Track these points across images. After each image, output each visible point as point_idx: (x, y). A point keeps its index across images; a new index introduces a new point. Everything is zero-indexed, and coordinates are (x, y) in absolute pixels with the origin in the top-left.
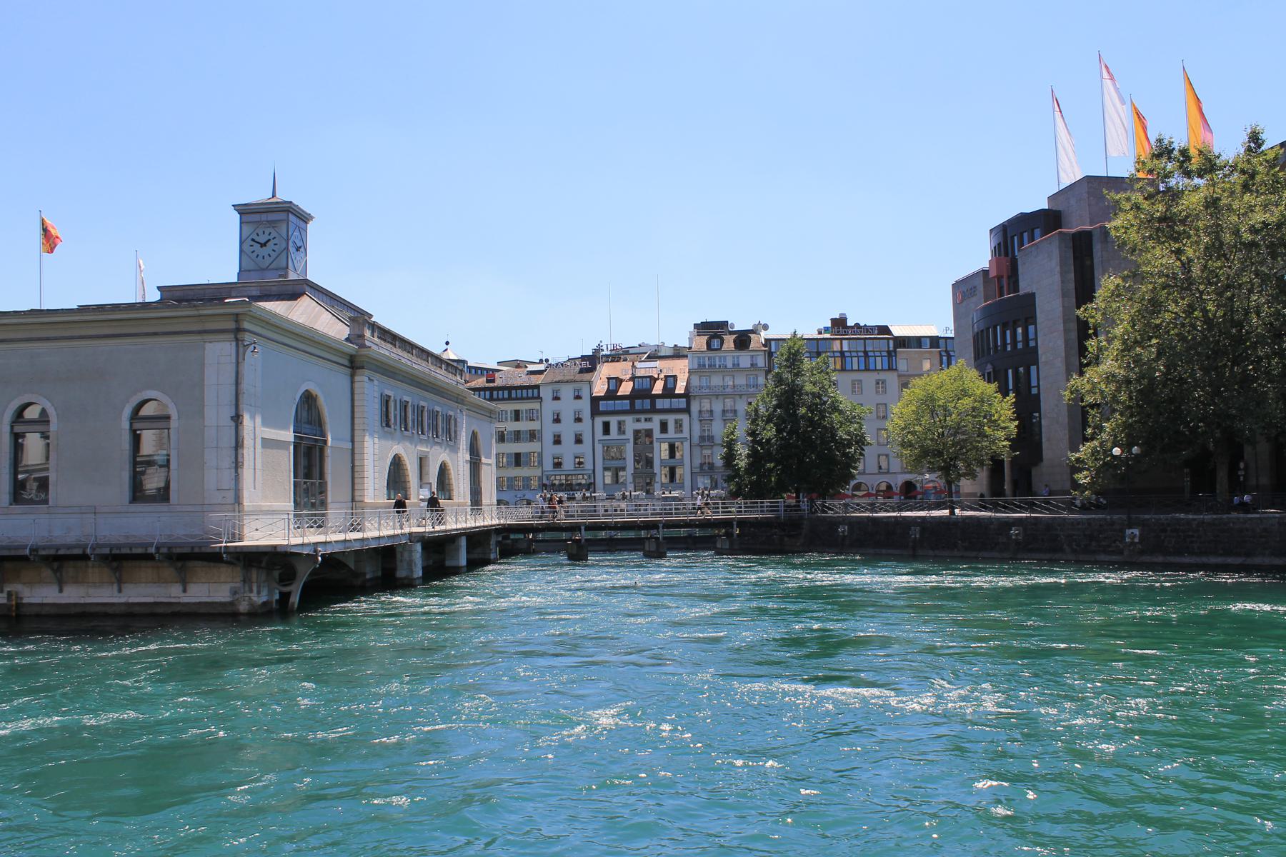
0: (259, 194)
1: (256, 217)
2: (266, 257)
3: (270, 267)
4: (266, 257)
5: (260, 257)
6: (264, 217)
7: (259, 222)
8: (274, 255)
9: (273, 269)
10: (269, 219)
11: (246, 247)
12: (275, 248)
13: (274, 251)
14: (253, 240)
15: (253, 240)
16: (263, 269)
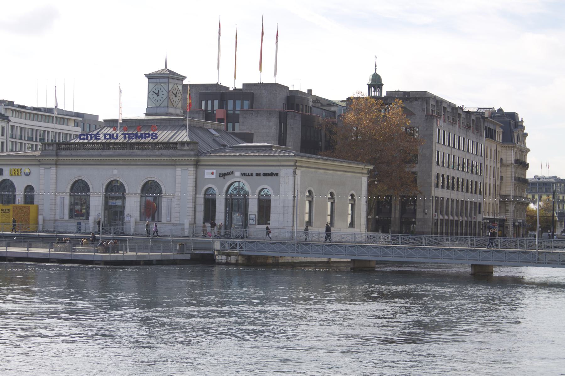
0: (157, 67)
1: (155, 80)
2: (159, 101)
3: (161, 106)
4: (159, 101)
5: (156, 101)
6: (158, 80)
7: (157, 83)
8: (162, 100)
9: (161, 107)
10: (160, 81)
11: (150, 94)
12: (163, 96)
13: (162, 98)
14: (153, 92)
15: (153, 92)
16: (157, 107)
